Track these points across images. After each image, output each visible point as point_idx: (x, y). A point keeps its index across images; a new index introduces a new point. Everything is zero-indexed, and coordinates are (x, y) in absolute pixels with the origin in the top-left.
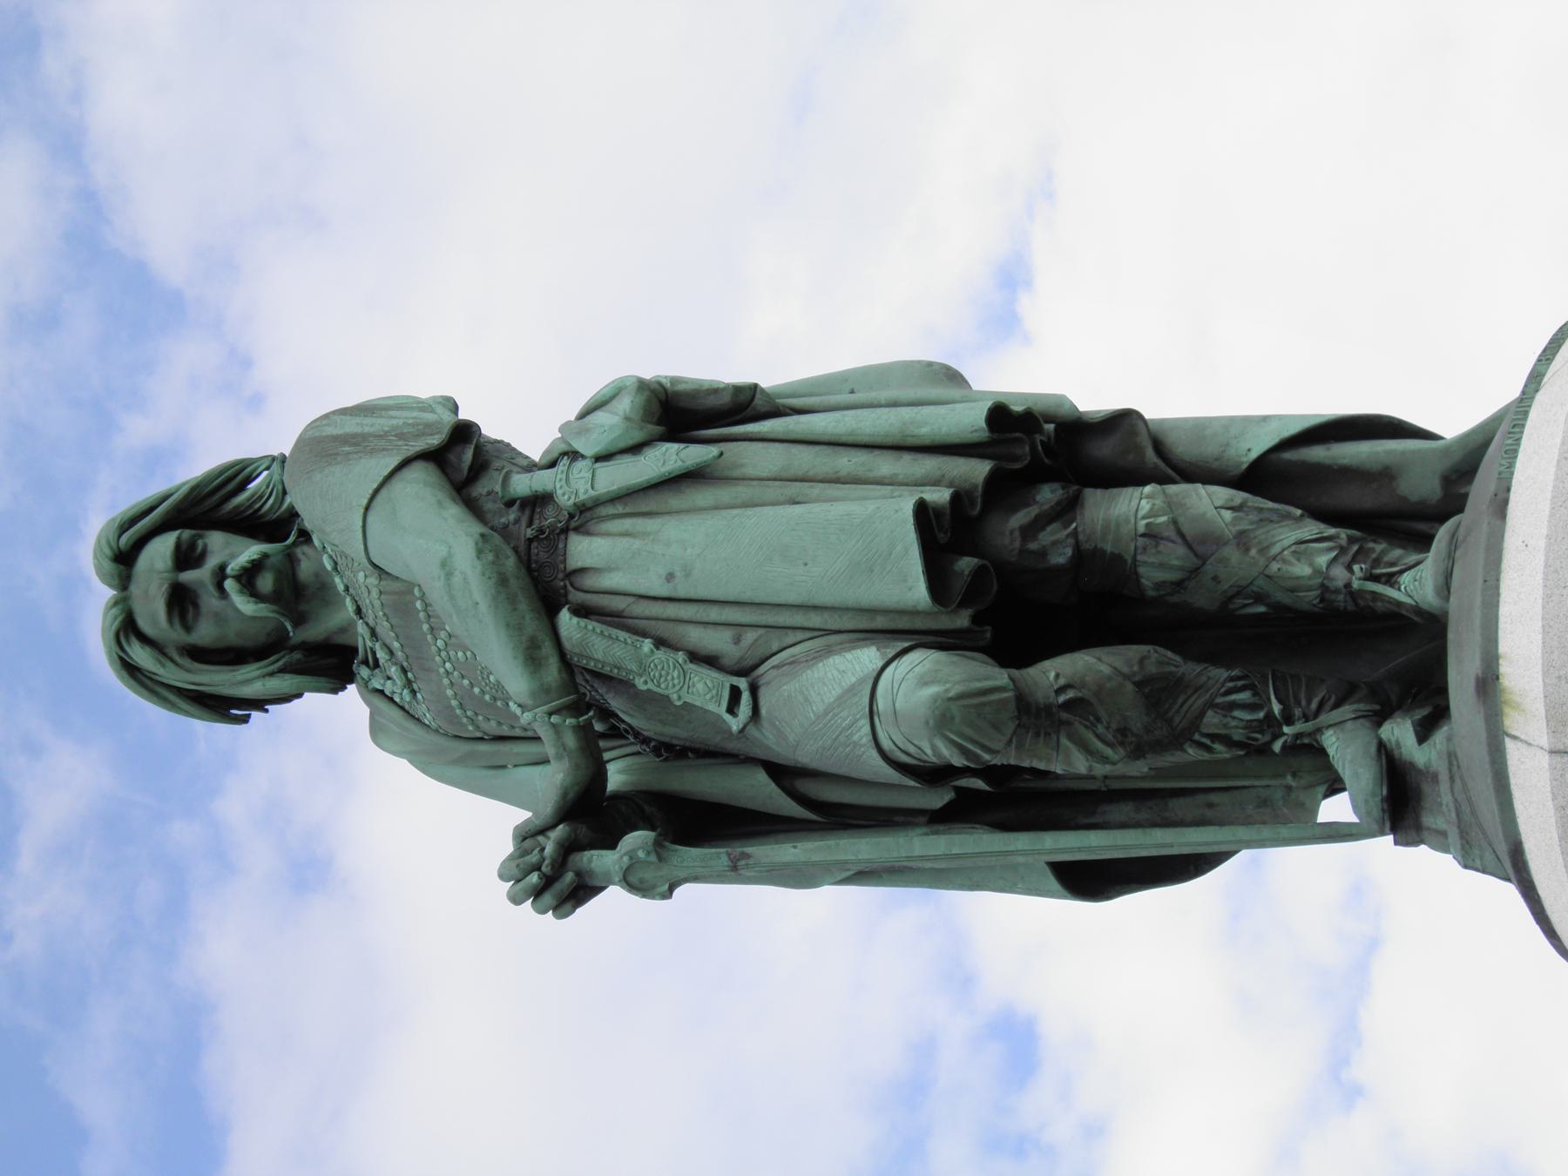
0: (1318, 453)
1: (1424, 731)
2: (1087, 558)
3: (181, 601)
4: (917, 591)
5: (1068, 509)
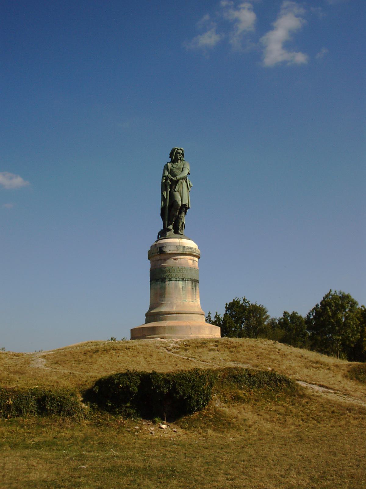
0: (183, 226)
1: (174, 232)
2: (182, 212)
3: (179, 153)
4: (184, 203)
5: (184, 212)
